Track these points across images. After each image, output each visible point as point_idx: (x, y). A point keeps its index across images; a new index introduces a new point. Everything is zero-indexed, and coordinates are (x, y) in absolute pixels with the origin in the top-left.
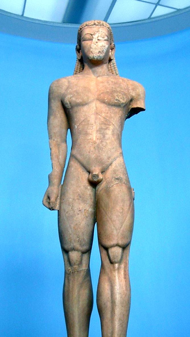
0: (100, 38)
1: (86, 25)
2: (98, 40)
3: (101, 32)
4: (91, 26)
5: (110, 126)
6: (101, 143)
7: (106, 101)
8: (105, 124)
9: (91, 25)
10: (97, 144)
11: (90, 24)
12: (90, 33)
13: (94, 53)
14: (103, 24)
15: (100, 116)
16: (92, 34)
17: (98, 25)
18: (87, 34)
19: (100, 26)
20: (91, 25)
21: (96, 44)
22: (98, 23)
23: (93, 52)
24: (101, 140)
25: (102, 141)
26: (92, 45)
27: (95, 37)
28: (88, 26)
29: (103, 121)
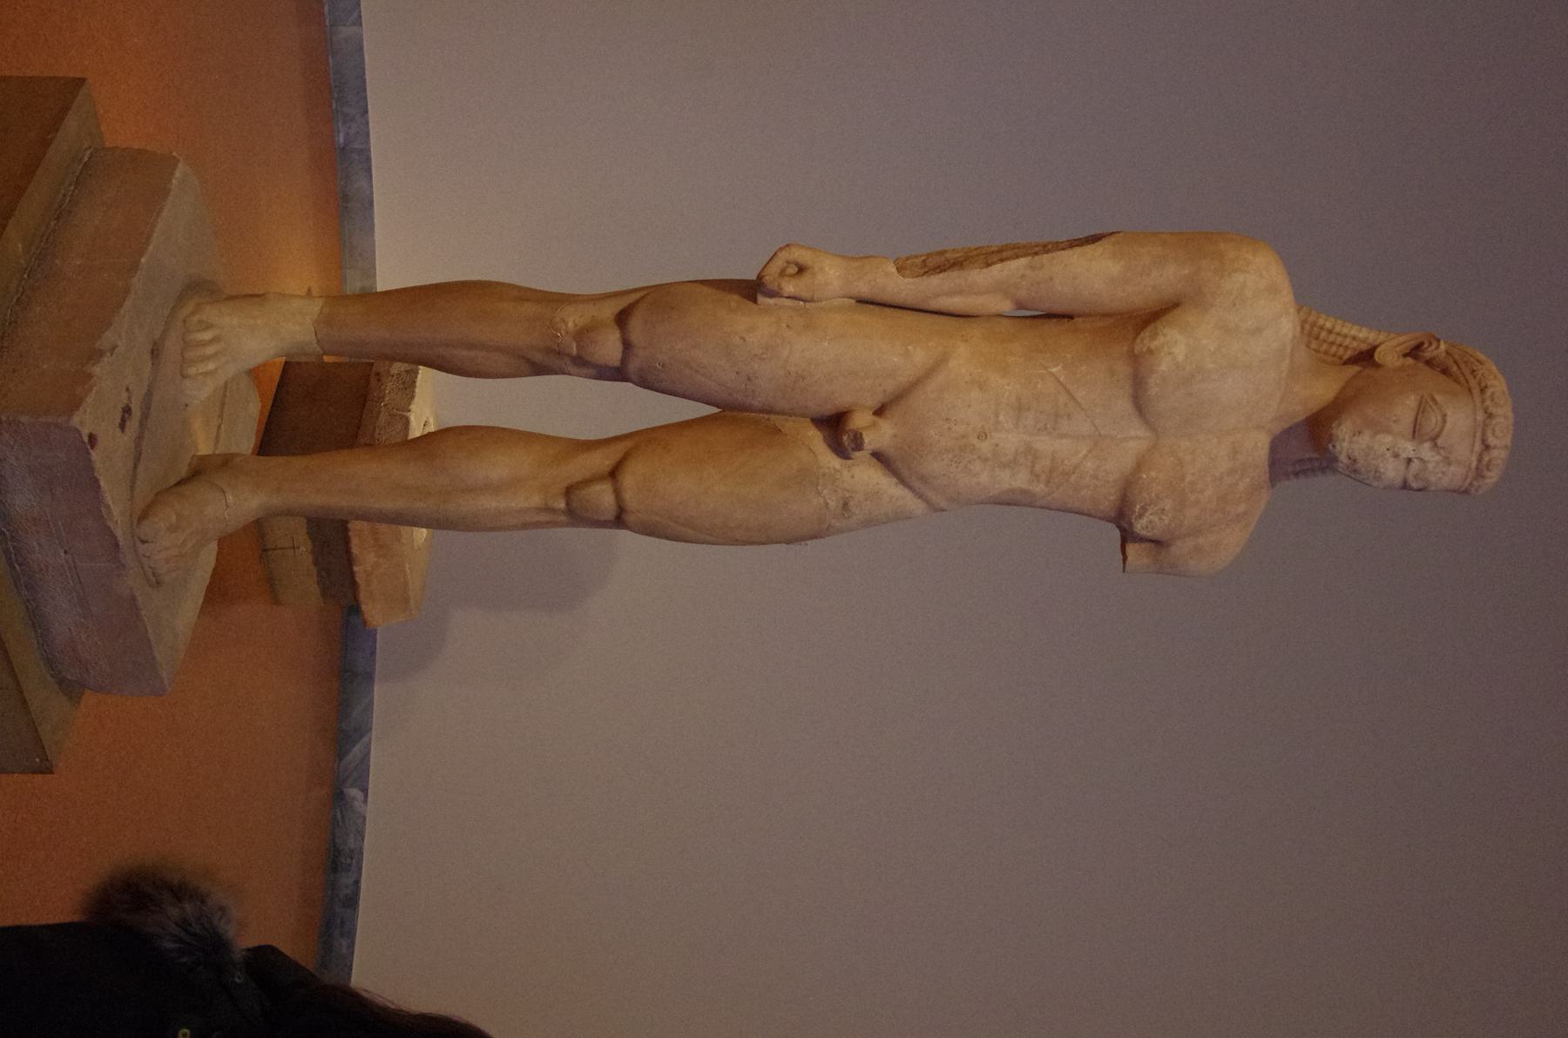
0: (1416, 465)
1: (1490, 416)
2: (1409, 460)
3: (1444, 470)
4: (1479, 435)
5: (1042, 486)
6: (979, 458)
7: (1144, 476)
8: (1052, 470)
9: (1484, 434)
10: (977, 446)
11: (1489, 433)
12: (1445, 432)
13: (1351, 442)
14: (1483, 477)
15: (1084, 452)
16: (1439, 442)
17: (1480, 460)
18: (1444, 421)
19: (1474, 464)
20: (1484, 434)
21: (1388, 454)
22: (1490, 461)
23: (1355, 439)
24: (989, 455)
25: (986, 460)
26: (1388, 439)
27: (1426, 451)
28: (1485, 425)
29: (1066, 462)
